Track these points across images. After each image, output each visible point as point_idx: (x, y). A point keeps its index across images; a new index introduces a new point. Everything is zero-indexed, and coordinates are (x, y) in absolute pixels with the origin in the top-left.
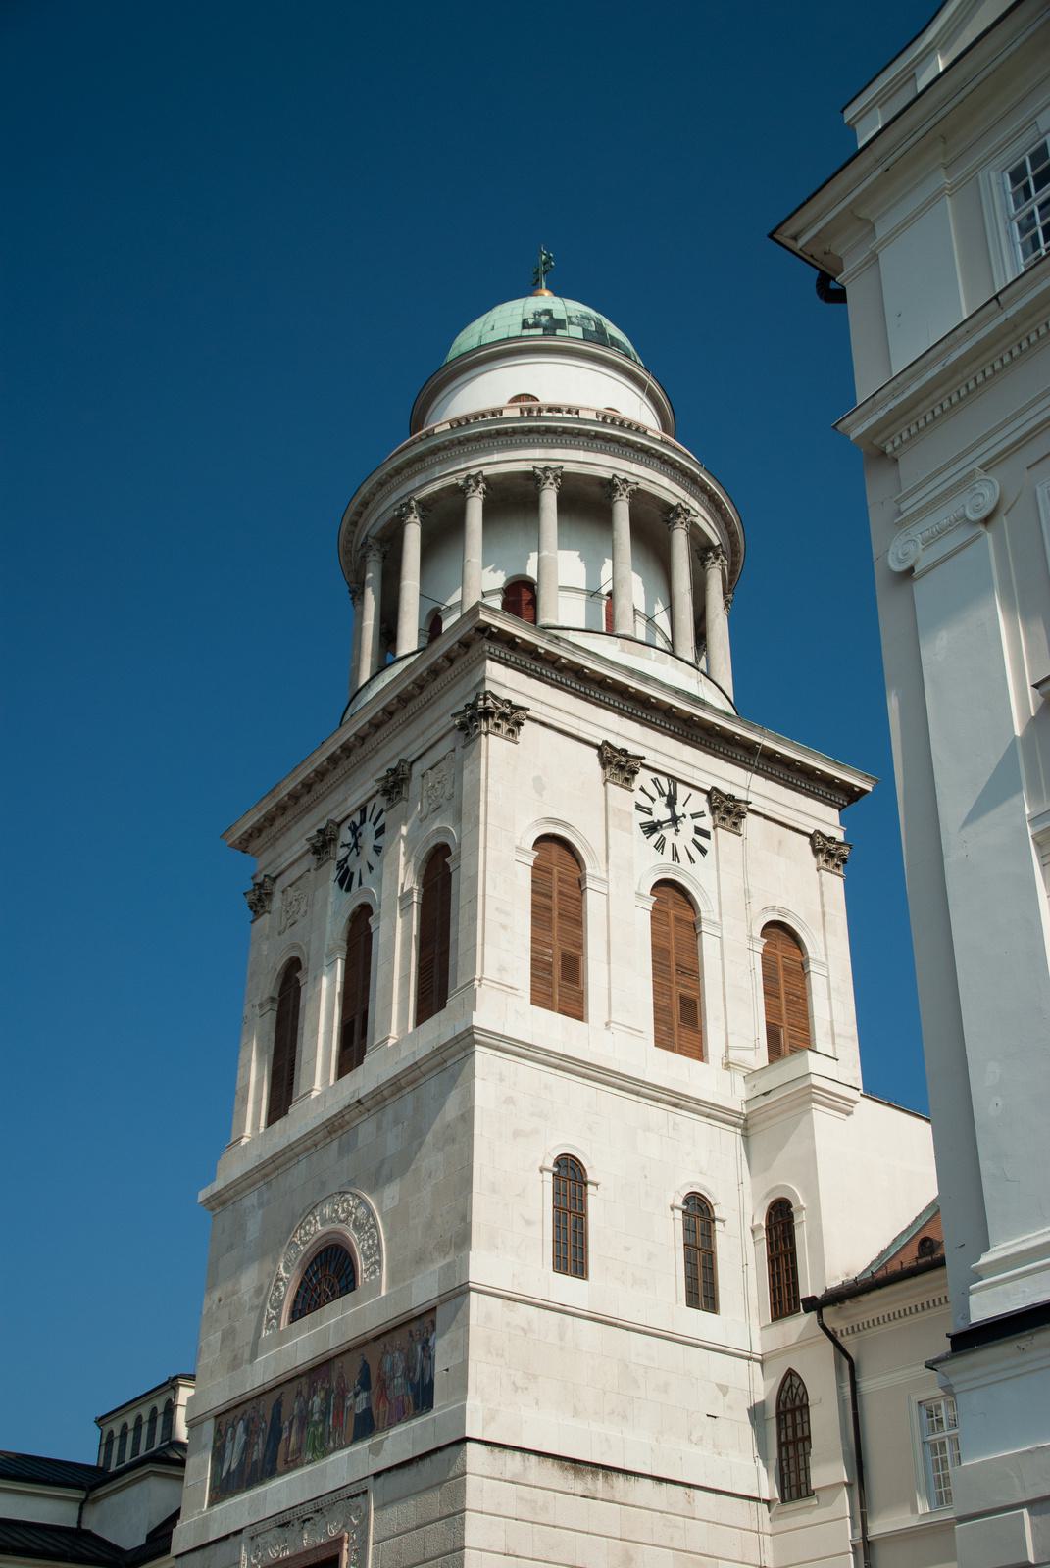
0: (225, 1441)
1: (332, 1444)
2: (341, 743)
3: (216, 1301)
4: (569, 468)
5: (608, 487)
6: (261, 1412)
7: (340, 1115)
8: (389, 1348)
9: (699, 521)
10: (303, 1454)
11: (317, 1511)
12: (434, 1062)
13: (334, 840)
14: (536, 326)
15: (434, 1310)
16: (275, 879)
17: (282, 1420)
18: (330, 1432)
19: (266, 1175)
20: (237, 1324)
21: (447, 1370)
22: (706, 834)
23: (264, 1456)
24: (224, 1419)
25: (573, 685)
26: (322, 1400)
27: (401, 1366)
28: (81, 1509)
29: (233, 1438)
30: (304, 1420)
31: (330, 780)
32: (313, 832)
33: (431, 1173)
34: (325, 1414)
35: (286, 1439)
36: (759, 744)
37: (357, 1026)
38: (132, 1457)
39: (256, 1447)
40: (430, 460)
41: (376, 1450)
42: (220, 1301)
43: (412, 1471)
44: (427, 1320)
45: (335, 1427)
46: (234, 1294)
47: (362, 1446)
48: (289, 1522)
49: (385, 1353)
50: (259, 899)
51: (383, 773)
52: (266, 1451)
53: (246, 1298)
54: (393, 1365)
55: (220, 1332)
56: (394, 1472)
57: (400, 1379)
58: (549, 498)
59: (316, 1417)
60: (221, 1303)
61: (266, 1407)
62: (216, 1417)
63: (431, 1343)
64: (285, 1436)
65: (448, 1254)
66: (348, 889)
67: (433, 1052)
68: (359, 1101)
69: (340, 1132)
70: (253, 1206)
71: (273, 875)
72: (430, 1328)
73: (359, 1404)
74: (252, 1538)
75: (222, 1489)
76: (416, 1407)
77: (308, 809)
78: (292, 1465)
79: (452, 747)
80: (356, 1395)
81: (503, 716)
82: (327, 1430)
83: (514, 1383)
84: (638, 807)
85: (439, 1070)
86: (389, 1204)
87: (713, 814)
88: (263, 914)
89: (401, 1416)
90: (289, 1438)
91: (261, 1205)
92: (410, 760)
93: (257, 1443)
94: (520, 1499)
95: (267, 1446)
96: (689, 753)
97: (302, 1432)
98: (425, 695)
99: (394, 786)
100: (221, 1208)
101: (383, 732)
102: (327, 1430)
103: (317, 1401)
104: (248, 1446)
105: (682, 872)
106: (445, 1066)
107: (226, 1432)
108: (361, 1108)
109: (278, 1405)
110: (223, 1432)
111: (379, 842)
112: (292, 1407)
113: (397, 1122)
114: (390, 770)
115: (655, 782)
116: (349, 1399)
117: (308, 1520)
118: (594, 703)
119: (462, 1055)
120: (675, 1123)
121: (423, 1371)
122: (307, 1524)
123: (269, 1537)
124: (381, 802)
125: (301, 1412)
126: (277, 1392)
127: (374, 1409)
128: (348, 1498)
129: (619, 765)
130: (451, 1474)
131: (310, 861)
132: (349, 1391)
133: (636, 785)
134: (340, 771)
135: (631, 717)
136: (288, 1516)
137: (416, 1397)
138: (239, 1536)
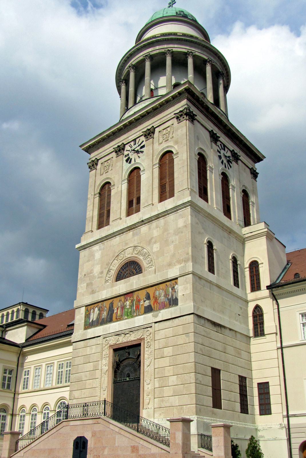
0: (90, 313)
3: (84, 275)
6: (105, 305)
8: (157, 289)
10: (123, 317)
11: (131, 332)
13: (123, 149)
15: (177, 279)
16: (98, 160)
17: (114, 307)
18: (134, 311)
19: (103, 241)
20: (93, 282)
21: (183, 295)
23: (107, 317)
24: (89, 307)
25: (205, 112)
26: (130, 303)
27: (163, 294)
28: (2, 332)
29: (94, 312)
30: (123, 308)
33: (173, 241)
34: (131, 306)
36: (243, 141)
38: (16, 319)
39: (103, 315)
41: (156, 316)
42: (85, 275)
43: (171, 321)
44: (173, 282)
45: (136, 310)
46: (91, 273)
47: (150, 315)
48: (120, 334)
49: (156, 290)
50: (93, 165)
52: (108, 315)
53: (96, 274)
54: (159, 294)
55: (86, 284)
56: (163, 322)
57: (163, 298)
59: (128, 307)
60: (86, 276)
61: (107, 304)
62: (86, 306)
63: (175, 288)
64: (115, 311)
65: (182, 263)
66: (130, 163)
68: (142, 221)
69: (133, 230)
70: (97, 250)
71: (98, 159)
72: (175, 284)
73: (147, 303)
74: (104, 338)
75: (89, 325)
76: (170, 305)
78: (118, 319)
79: (172, 124)
80: (144, 301)
82: (133, 310)
83: (202, 300)
86: (155, 250)
87: (232, 157)
88: (94, 169)
89: (164, 306)
90: (117, 312)
91: (100, 250)
92: (155, 127)
93: (104, 313)
94: (204, 331)
95: (108, 314)
97: (122, 311)
99: (149, 134)
102: (133, 310)
103: (128, 303)
104: (99, 314)
106: (177, 212)
107: (90, 310)
108: (143, 223)
109: (112, 305)
110: (89, 310)
112: (117, 303)
113: (157, 227)
114: (148, 129)
115: (221, 145)
116: (142, 302)
117: (128, 334)
118: (209, 119)
119: (185, 209)
120: (230, 237)
121: (172, 295)
122: (127, 335)
124: (143, 138)
125: (121, 305)
126: (111, 300)
128: (144, 328)
129: (214, 138)
132: (141, 300)
136: (119, 333)
137: (170, 302)
138: (99, 338)
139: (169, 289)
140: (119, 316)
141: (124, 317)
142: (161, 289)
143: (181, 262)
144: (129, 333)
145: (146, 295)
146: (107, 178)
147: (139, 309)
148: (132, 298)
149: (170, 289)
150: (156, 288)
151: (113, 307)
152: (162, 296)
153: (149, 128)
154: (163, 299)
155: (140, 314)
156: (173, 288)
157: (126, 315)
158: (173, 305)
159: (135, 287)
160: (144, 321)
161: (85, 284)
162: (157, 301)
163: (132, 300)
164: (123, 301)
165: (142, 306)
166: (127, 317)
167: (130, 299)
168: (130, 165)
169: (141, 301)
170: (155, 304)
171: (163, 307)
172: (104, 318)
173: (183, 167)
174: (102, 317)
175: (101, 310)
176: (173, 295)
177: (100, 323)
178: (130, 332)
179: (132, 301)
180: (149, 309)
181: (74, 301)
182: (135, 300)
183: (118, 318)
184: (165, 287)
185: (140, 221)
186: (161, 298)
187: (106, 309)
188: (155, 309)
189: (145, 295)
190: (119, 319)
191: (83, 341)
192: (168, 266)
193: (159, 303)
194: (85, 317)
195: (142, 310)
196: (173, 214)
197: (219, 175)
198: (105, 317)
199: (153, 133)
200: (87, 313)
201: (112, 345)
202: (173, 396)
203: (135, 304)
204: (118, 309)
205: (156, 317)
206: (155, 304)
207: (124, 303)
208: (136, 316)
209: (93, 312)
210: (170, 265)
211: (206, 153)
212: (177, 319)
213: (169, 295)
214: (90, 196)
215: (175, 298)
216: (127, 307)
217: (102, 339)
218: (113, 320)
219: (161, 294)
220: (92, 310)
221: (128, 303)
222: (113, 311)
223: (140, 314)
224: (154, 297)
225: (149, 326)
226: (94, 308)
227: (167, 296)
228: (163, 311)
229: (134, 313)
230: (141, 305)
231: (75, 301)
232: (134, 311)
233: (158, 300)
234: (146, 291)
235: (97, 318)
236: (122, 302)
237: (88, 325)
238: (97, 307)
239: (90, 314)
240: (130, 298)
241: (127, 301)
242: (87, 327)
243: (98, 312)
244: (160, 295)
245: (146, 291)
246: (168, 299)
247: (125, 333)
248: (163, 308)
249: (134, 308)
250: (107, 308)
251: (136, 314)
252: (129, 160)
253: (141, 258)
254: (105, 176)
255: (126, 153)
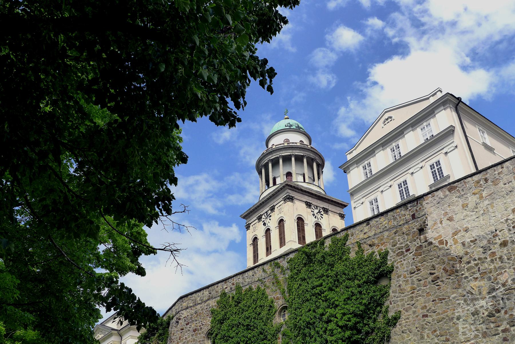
4: (296, 154)
5: (303, 157)
9: (318, 161)
13: (261, 218)
14: (287, 126)
22: (322, 215)
31: (260, 207)
37: (269, 248)
40: (273, 152)
50: (248, 227)
58: (293, 159)
66: (265, 226)
77: (256, 212)
81: (291, 198)
84: (312, 211)
96: (319, 202)
99: (272, 209)
105: (319, 221)
111: (270, 218)
115: (314, 207)
124: (270, 211)
129: (309, 205)
131: (257, 221)
133: (311, 208)
134: (262, 206)
135: (310, 196)
146: (256, 235)
168: (265, 227)
197: (313, 226)
199: (274, 208)
211: (303, 216)
214: (248, 245)
254: (254, 234)
255: (263, 220)
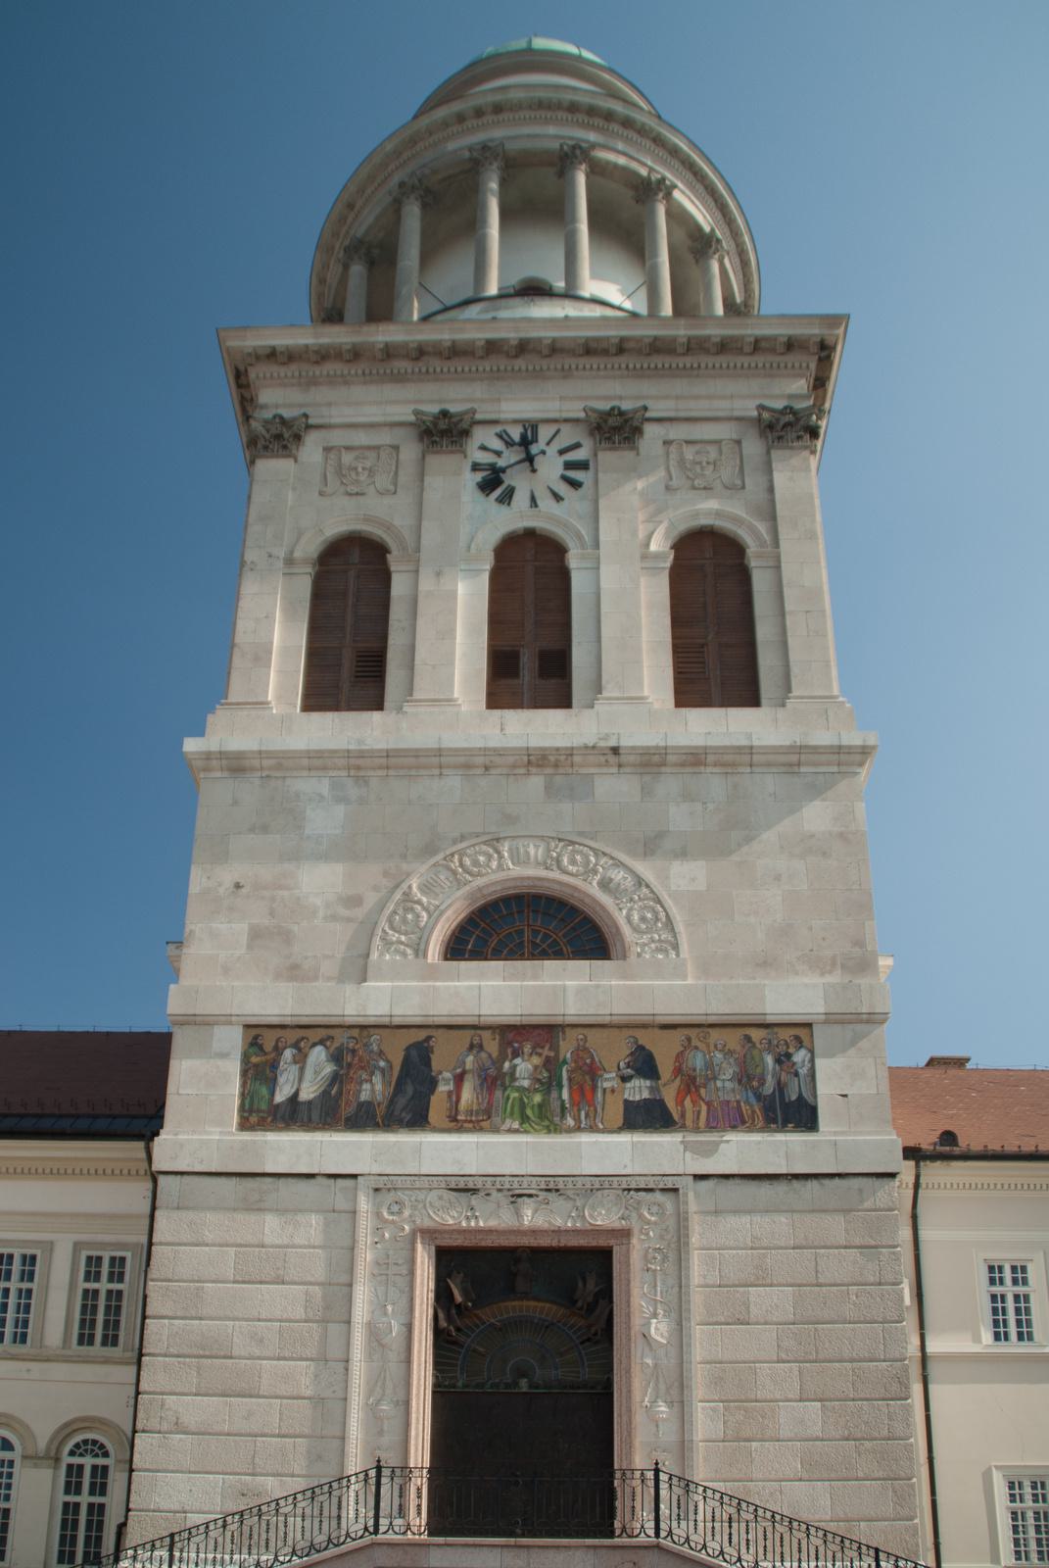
1: (570, 1122)
2: (523, 335)
7: (570, 752)
8: (694, 1042)
12: (783, 759)
15: (809, 1025)
18: (563, 1108)
20: (295, 928)
21: (845, 1096)
26: (536, 1068)
27: (729, 1071)
29: (301, 1059)
32: (434, 409)
34: (548, 1082)
35: (450, 1093)
39: (366, 1086)
41: (709, 1150)
42: (238, 886)
43: (781, 1188)
46: (281, 887)
51: (605, 406)
54: (709, 1065)
56: (738, 1181)
57: (729, 1085)
62: (247, 1027)
64: (443, 1088)
65: (830, 972)
67: (791, 747)
68: (615, 750)
72: (792, 1045)
73: (638, 1090)
74: (377, 1190)
80: (625, 1079)
82: (555, 1105)
85: (783, 769)
98: (688, 361)
100: (226, 774)
101: (594, 361)
103: (524, 1068)
106: (796, 769)
107: (278, 1050)
108: (612, 759)
117: (530, 1196)
121: (780, 1087)
123: (433, 1196)
127: (671, 1104)
130: (867, 1205)
139: (762, 1059)
140: (470, 1112)
141: (503, 1123)
142: (716, 1046)
143: (828, 968)
144: (537, 1196)
145: (632, 1054)
147: (592, 1103)
148: (546, 1052)
149: (769, 1060)
150: (689, 1039)
151: (428, 1063)
152: (724, 1077)
153: (626, 406)
154: (733, 1090)
155: (601, 1126)
156: (785, 1058)
157: (512, 1114)
158: (784, 1125)
159: (573, 1008)
160: (632, 1160)
161: (241, 928)
162: (697, 1090)
163: (547, 1057)
164: (495, 1055)
165: (608, 1095)
166: (521, 1124)
167: (540, 1055)
169: (606, 1076)
170: (688, 1102)
171: (733, 1123)
172: (369, 1104)
173: (807, 612)
174: (360, 1092)
175: (349, 1065)
176: (786, 1084)
177: (348, 1119)
178: (541, 1190)
179: (552, 1065)
180: (649, 1116)
181: (168, 986)
182: (565, 1062)
183: (459, 1118)
184: (743, 1047)
185: (602, 744)
186: (719, 1084)
187: (382, 1064)
188: (689, 1123)
189: (628, 1052)
190: (466, 1125)
191: (234, 1181)
192: (757, 965)
193: (708, 1104)
194: (244, 1073)
195: (615, 1113)
196: (774, 770)
198: (379, 1098)
200: (254, 1060)
201: (435, 1231)
202: (801, 1480)
203: (570, 1080)
204: (459, 1079)
205: (708, 1156)
206: (688, 1102)
207: (498, 1063)
208: (578, 1129)
209: (295, 1062)
210: (766, 963)
212: (813, 1184)
213: (762, 1082)
215: (794, 1097)
216: (517, 1084)
217: (371, 1191)
218: (430, 1119)
219: (717, 1068)
220: (288, 1054)
221: (524, 1068)
222: (433, 1083)
223: (601, 1126)
224: (678, 1071)
225: (661, 1186)
226: (302, 1044)
227: (755, 1084)
228: (734, 1138)
229: (563, 1116)
230: (604, 1090)
231: (172, 986)
232: (563, 1108)
233: (703, 1091)
234: (632, 1040)
235: (325, 1093)
236: (483, 1055)
237: (259, 1111)
238: (322, 1042)
239: (274, 1065)
240: (539, 1050)
241: (516, 1054)
242: (254, 1119)
243: (329, 1069)
244: (713, 1070)
245: (632, 1040)
246: (759, 1097)
247: (509, 1190)
248: (734, 1127)
249: (565, 1095)
250: (388, 1061)
251: (577, 1120)
252: (492, 482)
253: (606, 900)
